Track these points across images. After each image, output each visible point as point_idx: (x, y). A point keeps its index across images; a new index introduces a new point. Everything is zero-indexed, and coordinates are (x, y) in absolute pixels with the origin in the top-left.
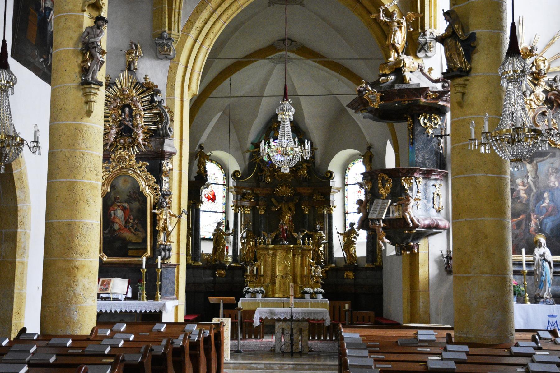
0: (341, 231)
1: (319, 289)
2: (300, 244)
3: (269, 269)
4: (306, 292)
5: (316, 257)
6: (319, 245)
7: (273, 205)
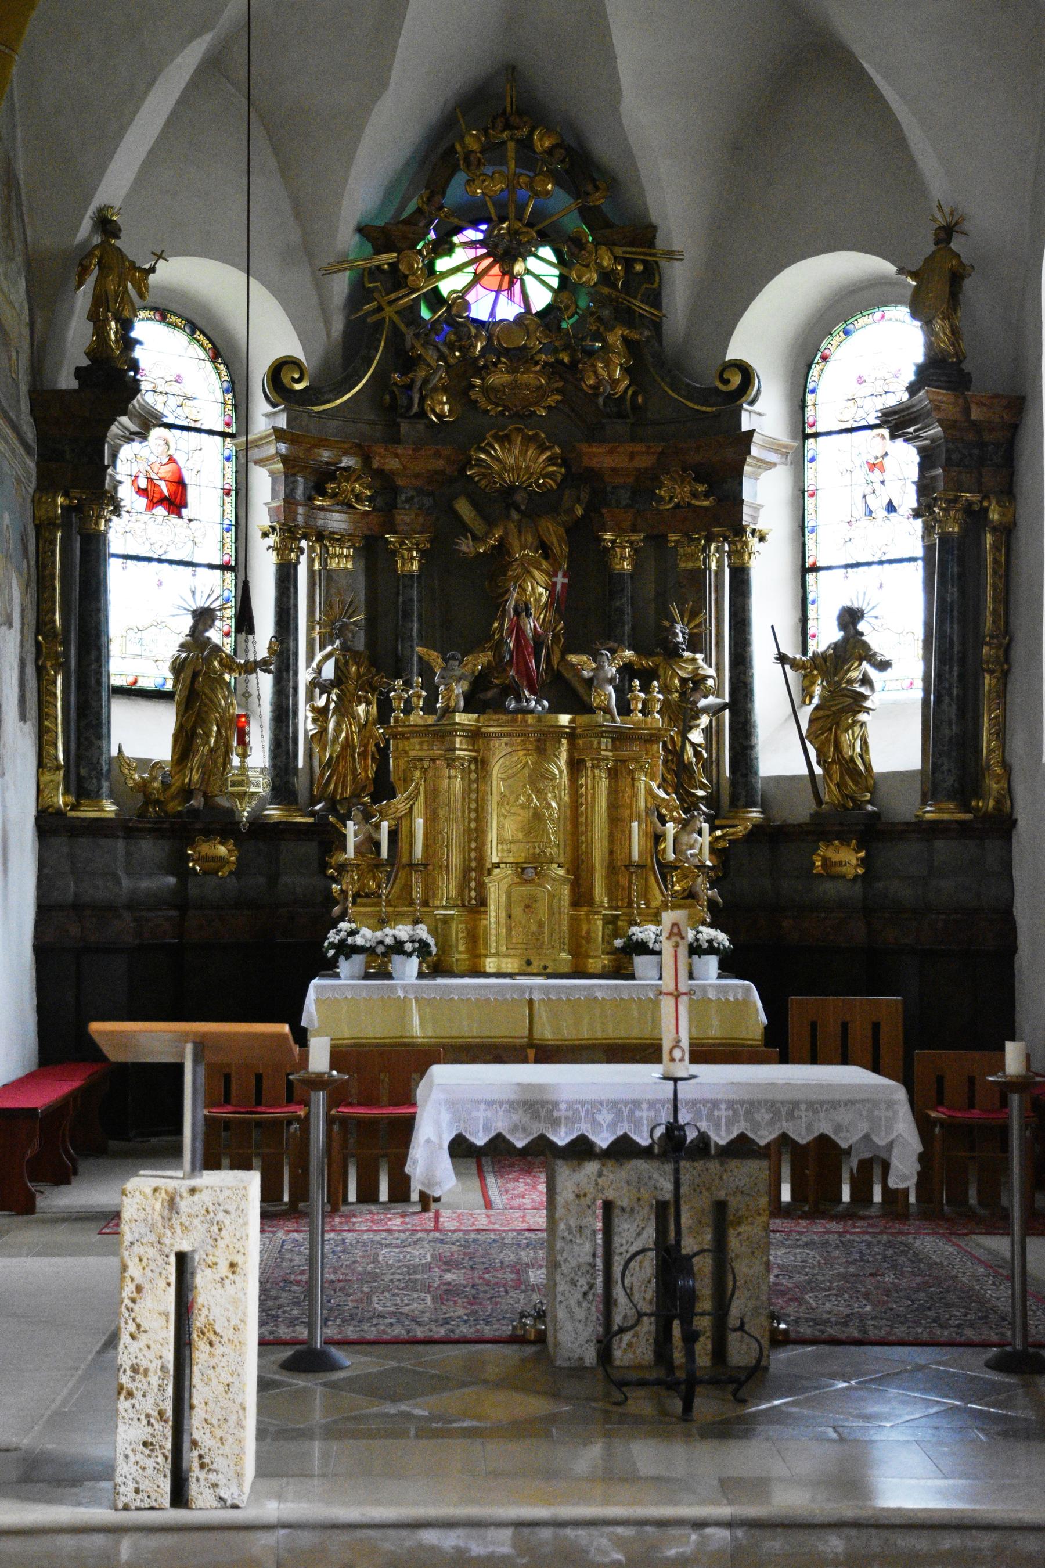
0: (791, 650)
1: (708, 933)
2: (607, 710)
3: (454, 832)
5: (679, 775)
6: (683, 714)
7: (464, 529)
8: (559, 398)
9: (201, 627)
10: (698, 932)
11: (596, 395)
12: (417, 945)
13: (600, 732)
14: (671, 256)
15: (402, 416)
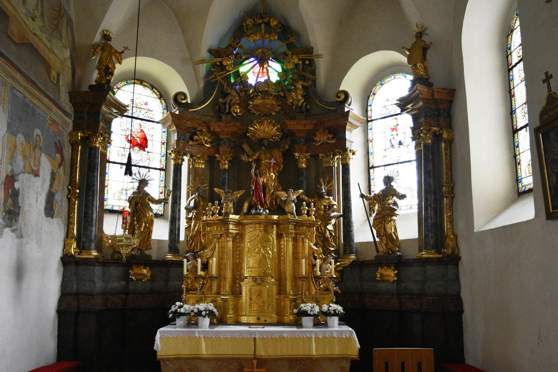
1: (334, 306)
2: (292, 213)
4: (305, 314)
5: (323, 241)
6: (326, 220)
7: (244, 152)
8: (280, 108)
9: (141, 186)
10: (330, 306)
11: (292, 105)
12: (208, 312)
13: (288, 222)
14: (318, 56)
15: (223, 113)
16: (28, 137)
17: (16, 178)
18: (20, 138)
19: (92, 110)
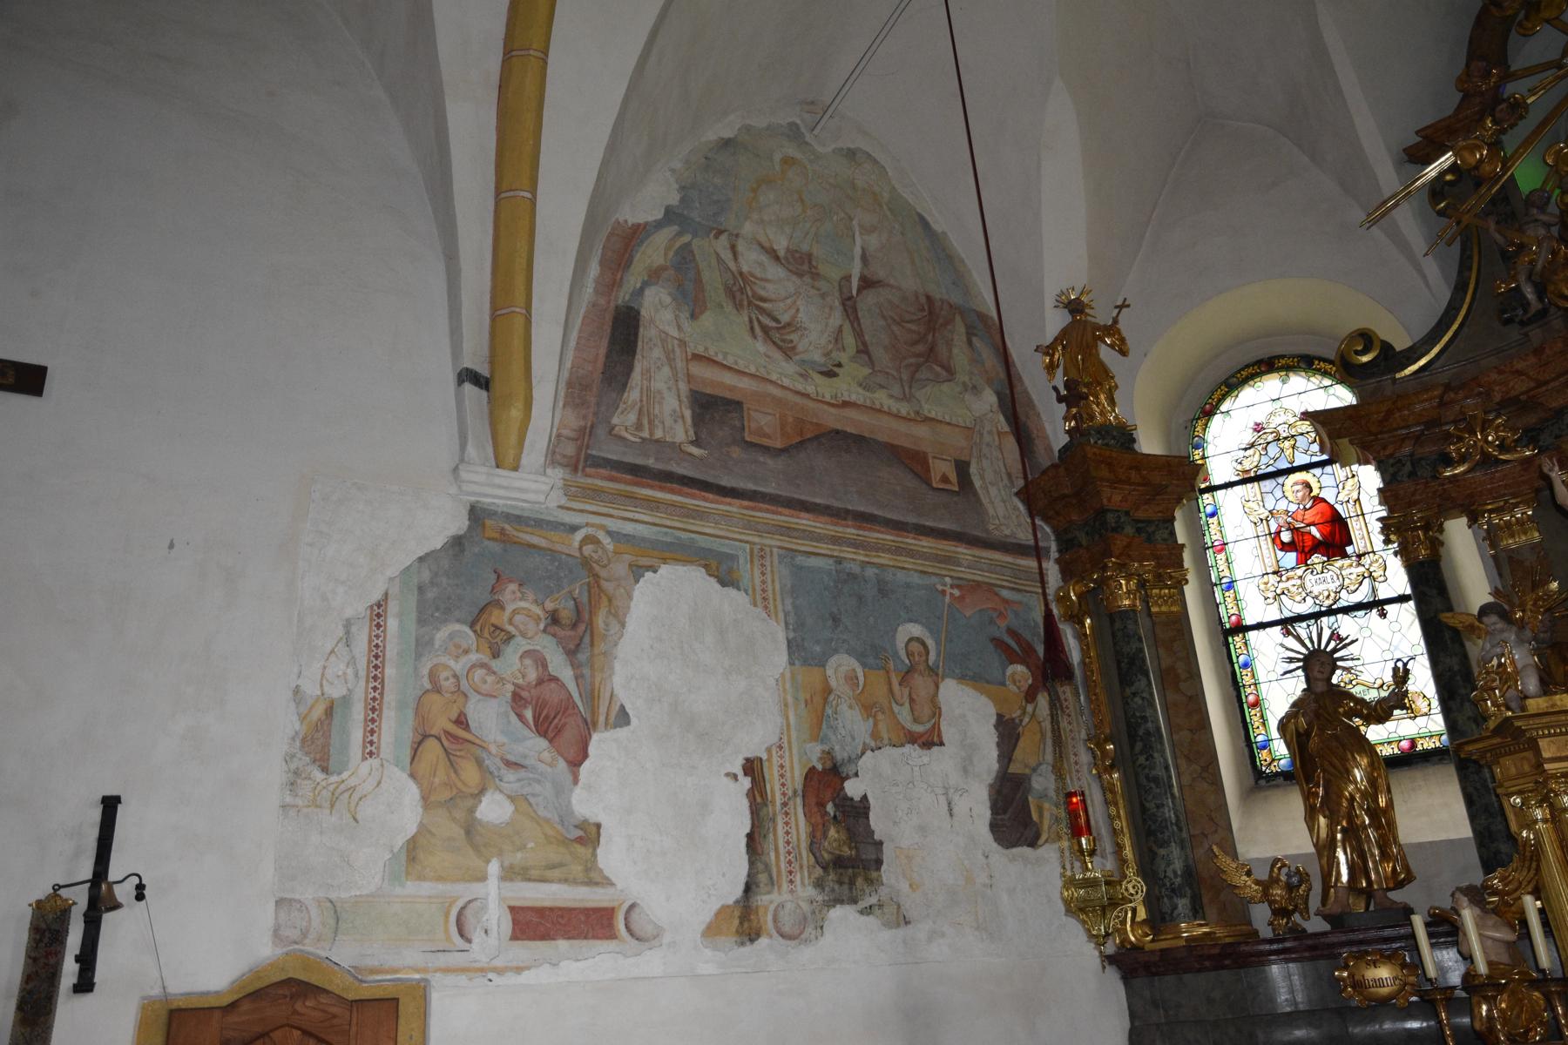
16: (874, 654)
17: (844, 770)
18: (841, 666)
19: (1117, 510)
